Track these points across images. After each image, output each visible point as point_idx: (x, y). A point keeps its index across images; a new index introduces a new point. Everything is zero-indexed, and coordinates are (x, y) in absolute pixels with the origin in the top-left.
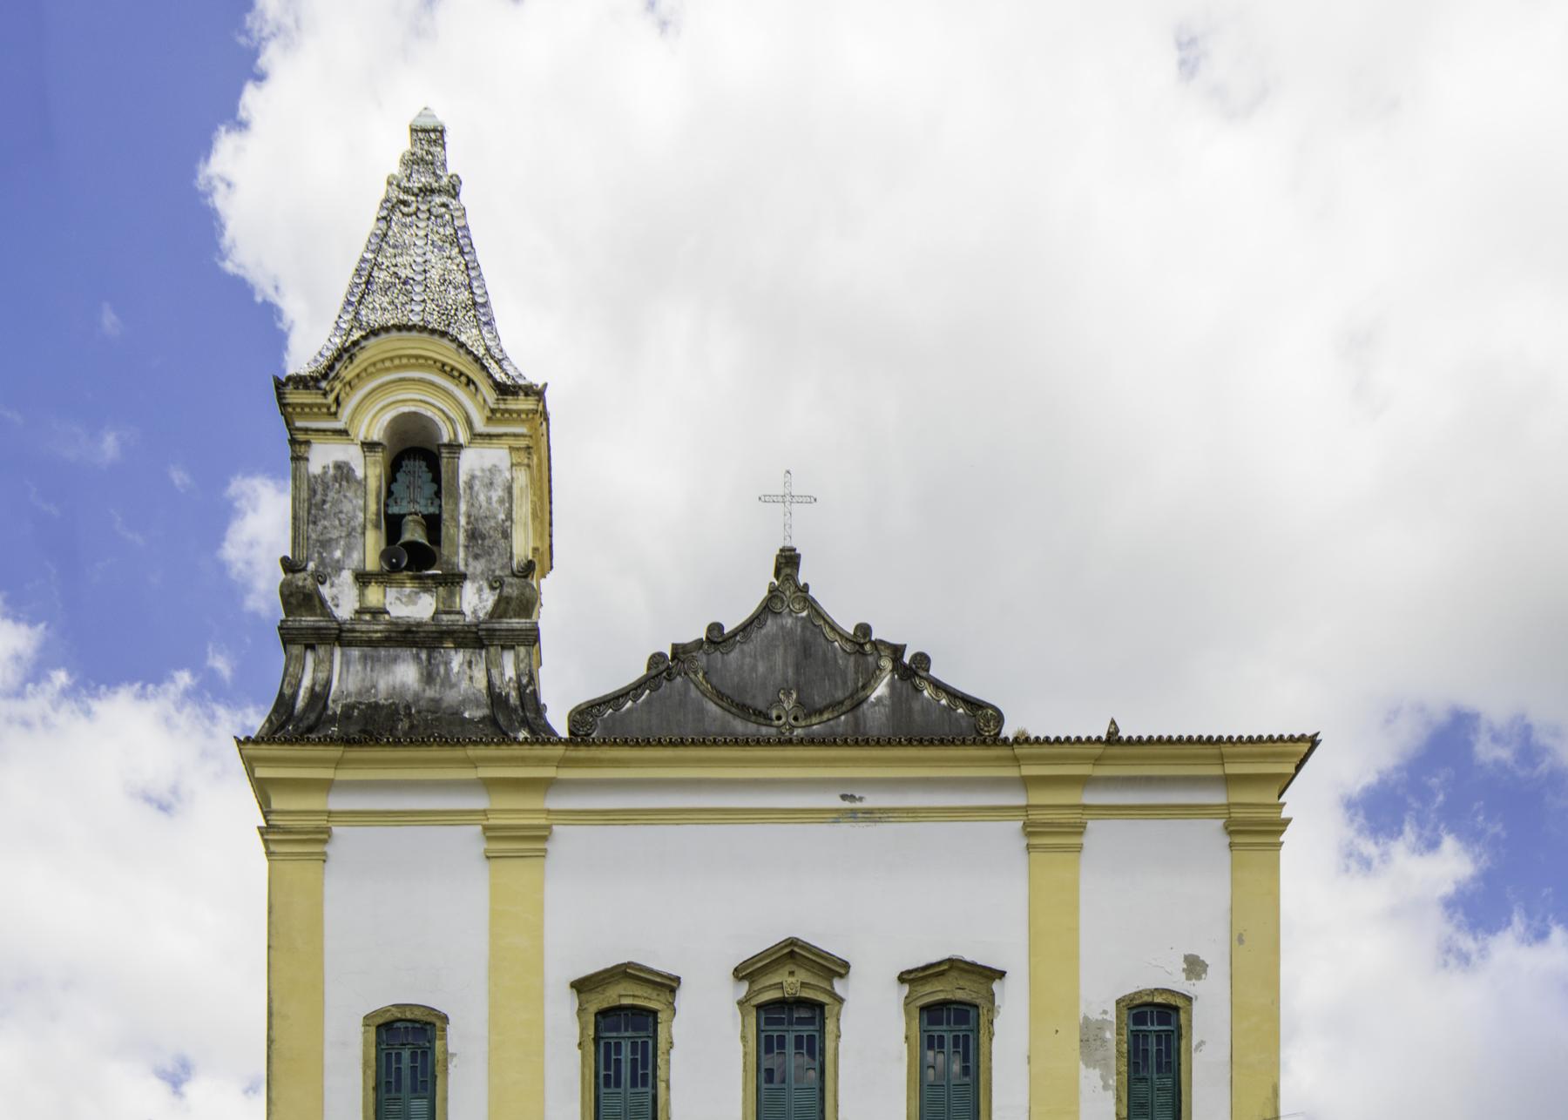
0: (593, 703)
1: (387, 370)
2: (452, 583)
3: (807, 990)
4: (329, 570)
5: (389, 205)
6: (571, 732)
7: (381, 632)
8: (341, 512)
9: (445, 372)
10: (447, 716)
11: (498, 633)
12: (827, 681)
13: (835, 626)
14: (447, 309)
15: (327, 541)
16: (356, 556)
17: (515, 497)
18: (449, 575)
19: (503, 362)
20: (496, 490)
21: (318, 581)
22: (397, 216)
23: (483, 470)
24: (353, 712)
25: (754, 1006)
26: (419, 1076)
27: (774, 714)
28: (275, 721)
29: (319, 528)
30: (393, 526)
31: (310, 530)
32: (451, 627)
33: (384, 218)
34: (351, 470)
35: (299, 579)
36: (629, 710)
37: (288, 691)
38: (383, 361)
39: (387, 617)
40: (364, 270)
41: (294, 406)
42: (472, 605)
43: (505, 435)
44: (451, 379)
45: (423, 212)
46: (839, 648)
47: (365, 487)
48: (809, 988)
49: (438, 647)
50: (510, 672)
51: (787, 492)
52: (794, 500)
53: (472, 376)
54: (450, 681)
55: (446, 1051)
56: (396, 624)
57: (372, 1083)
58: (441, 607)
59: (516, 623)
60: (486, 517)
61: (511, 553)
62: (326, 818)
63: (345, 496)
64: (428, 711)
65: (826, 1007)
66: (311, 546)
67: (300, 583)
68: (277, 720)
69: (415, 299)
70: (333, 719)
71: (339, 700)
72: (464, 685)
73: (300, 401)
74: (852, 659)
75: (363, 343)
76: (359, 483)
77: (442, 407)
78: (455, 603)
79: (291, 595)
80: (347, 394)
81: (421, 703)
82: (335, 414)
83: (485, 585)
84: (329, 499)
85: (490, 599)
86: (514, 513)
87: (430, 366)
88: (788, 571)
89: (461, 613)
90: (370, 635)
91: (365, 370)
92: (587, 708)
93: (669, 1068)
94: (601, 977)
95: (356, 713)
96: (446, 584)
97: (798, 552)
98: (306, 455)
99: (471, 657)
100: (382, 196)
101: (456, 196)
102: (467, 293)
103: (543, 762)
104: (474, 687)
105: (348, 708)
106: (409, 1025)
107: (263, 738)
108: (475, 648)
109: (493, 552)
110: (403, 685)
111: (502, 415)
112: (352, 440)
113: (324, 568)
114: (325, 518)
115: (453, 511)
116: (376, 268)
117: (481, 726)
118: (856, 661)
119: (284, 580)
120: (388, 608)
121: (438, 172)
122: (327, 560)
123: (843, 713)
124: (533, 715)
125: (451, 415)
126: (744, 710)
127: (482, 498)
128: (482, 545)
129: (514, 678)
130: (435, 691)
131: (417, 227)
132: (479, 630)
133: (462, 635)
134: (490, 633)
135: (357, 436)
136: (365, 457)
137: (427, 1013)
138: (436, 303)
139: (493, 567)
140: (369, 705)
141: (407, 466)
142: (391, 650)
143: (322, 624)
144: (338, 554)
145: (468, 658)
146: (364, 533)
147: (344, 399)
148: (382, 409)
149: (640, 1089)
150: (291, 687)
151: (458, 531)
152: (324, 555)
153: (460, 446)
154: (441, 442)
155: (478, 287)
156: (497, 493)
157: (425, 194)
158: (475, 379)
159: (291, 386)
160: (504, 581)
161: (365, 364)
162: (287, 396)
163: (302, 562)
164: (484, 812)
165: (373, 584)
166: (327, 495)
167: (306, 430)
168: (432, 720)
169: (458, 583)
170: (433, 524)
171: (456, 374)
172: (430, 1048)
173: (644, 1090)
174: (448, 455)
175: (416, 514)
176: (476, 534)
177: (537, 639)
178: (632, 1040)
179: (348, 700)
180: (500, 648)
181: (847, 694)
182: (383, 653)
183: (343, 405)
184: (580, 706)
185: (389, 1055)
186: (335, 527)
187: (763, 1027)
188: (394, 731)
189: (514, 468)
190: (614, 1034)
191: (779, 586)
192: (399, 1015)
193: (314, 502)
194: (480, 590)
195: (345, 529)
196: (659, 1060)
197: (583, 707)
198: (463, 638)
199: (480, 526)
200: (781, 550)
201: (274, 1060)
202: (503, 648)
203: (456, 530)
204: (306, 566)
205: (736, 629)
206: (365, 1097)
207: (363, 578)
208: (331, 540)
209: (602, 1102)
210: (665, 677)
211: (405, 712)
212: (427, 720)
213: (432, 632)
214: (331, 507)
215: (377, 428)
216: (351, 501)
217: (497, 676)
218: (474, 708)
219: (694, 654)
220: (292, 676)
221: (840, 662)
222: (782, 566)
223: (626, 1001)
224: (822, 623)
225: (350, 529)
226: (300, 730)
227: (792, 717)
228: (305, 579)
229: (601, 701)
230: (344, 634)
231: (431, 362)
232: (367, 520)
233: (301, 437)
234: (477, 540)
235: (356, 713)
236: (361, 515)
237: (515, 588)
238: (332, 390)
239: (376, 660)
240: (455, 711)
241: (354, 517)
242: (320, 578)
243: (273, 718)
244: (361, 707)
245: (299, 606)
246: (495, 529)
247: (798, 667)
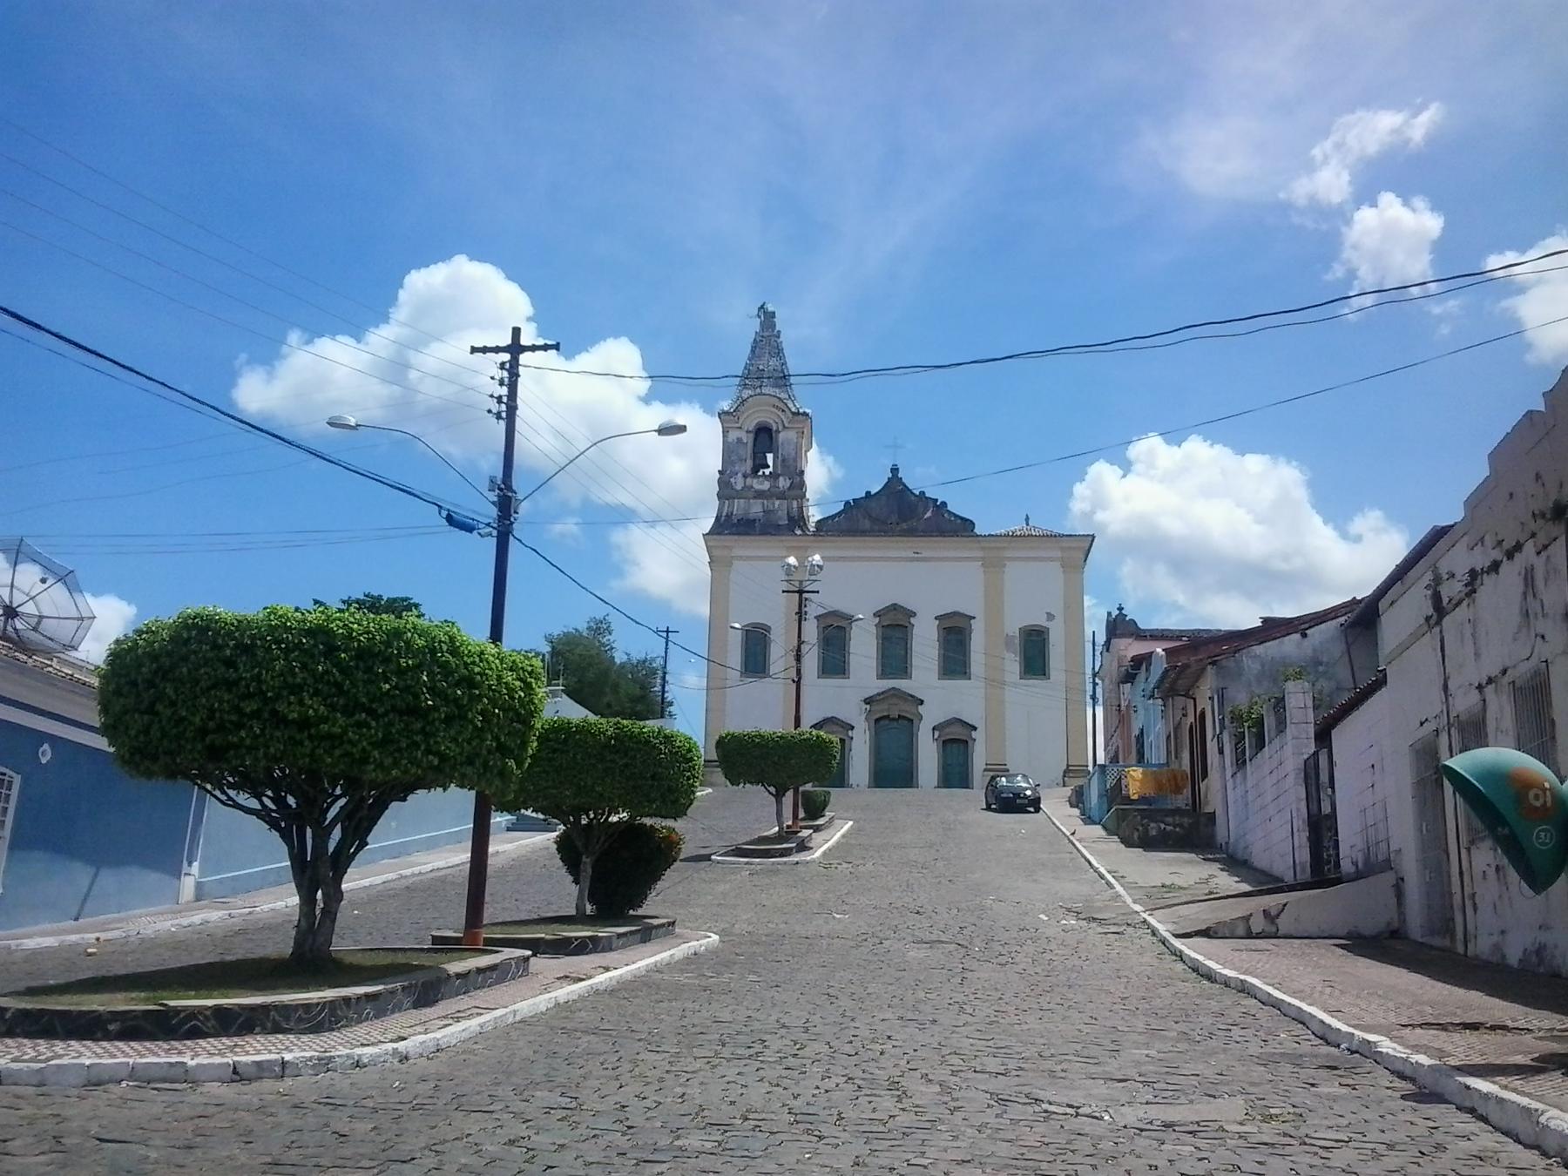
89: (778, 487)
194: (785, 480)
207: (745, 476)
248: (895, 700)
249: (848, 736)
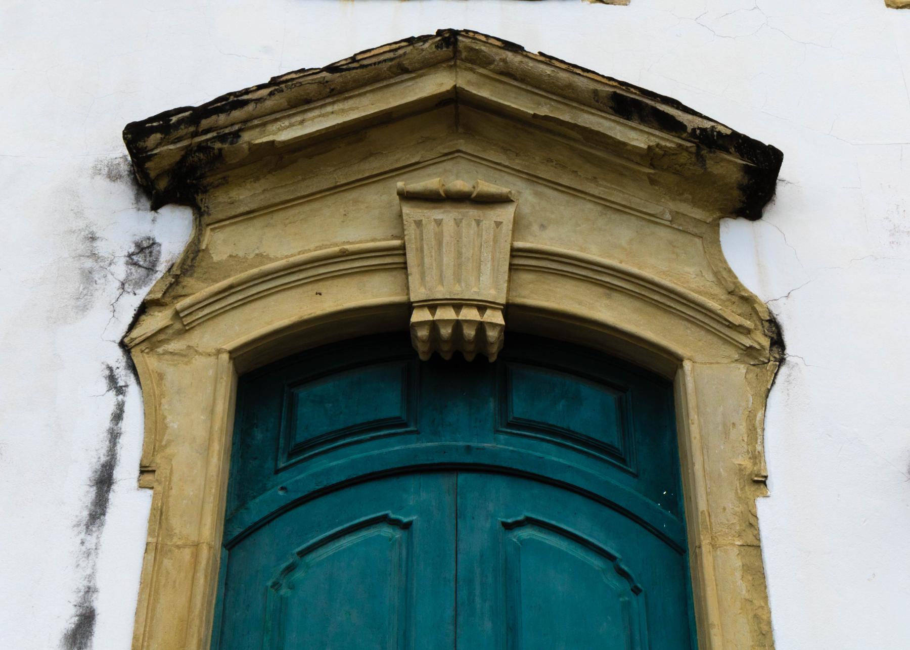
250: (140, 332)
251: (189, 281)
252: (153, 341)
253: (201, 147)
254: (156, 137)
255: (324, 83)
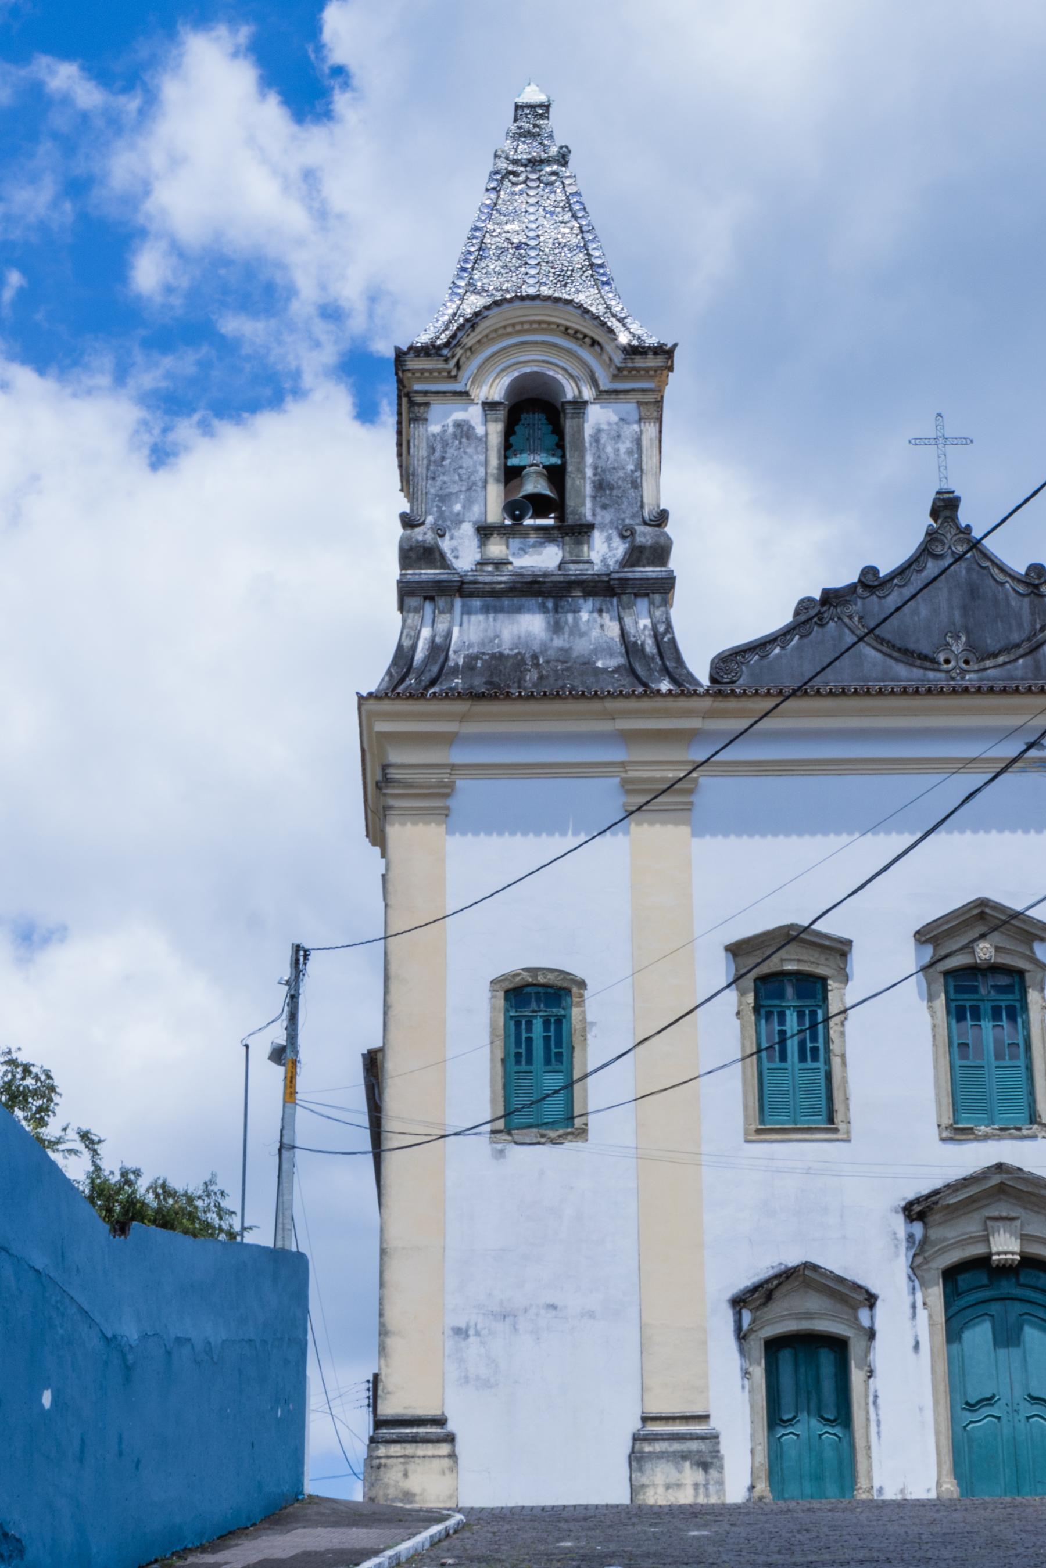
0: (738, 650)
1: (509, 334)
2: (580, 533)
3: (1003, 955)
4: (449, 523)
5: (498, 177)
6: (713, 680)
7: (505, 583)
8: (461, 467)
9: (568, 334)
10: (578, 666)
11: (631, 582)
12: (999, 623)
13: (1005, 568)
14: (562, 271)
15: (446, 495)
16: (476, 510)
17: (644, 449)
18: (577, 525)
19: (626, 321)
20: (624, 442)
21: (438, 534)
22: (506, 183)
23: (609, 424)
24: (476, 663)
25: (940, 972)
26: (553, 1046)
27: (941, 658)
28: (396, 675)
29: (438, 483)
30: (511, 475)
31: (428, 486)
32: (580, 577)
33: (494, 189)
34: (471, 428)
35: (420, 534)
36: (778, 656)
37: (407, 643)
38: (505, 327)
39: (510, 567)
40: (476, 238)
41: (413, 372)
42: (601, 554)
43: (633, 390)
44: (574, 340)
45: (533, 180)
46: (1010, 589)
47: (486, 443)
48: (1005, 953)
49: (566, 596)
50: (645, 622)
51: (940, 434)
52: (948, 443)
53: (596, 337)
54: (579, 630)
55: (584, 1020)
56: (521, 575)
57: (500, 1054)
58: (568, 558)
59: (650, 571)
60: (614, 468)
61: (642, 502)
62: (449, 771)
63: (465, 453)
64: (557, 661)
65: (1027, 975)
66: (430, 501)
67: (420, 538)
68: (397, 673)
69: (529, 262)
70: (455, 671)
71: (460, 651)
72: (595, 633)
73: (421, 367)
74: (1026, 600)
75: (486, 313)
76: (480, 439)
77: (564, 365)
78: (582, 551)
79: (411, 549)
80: (468, 358)
81: (549, 653)
82: (455, 377)
83: (614, 534)
84: (448, 455)
85: (620, 549)
86: (644, 463)
87: (552, 330)
88: (947, 513)
89: (589, 562)
90: (494, 586)
91: (487, 336)
92: (731, 655)
93: (844, 1041)
94: (760, 940)
95: (479, 664)
96: (573, 534)
97: (956, 494)
98: (425, 415)
99: (601, 605)
100: (491, 169)
101: (565, 164)
102: (581, 255)
103: (688, 713)
104: (606, 635)
105: (471, 659)
106: (541, 990)
107: (386, 694)
108: (605, 596)
109: (623, 502)
110: (529, 634)
111: (630, 372)
112: (473, 400)
113: (443, 522)
114: (444, 474)
115: (579, 463)
116: (487, 235)
117: (616, 676)
118: (1031, 603)
119: (403, 534)
120: (511, 559)
121: (546, 142)
122: (447, 514)
123: (1021, 657)
124: (674, 665)
125: (575, 373)
126: (908, 655)
127: (609, 449)
128: (610, 495)
129: (650, 626)
130: (564, 641)
131: (528, 195)
132: (611, 579)
133: (592, 584)
134: (623, 582)
135: (478, 396)
136: (486, 415)
137: (562, 977)
138: (551, 265)
139: (623, 516)
140: (493, 656)
141: (526, 419)
142: (516, 600)
143: (443, 577)
144: (458, 507)
145: (598, 605)
146: (485, 487)
147: (464, 363)
148: (503, 370)
149: (810, 1064)
150: (410, 639)
151: (585, 481)
152: (444, 508)
153: (585, 403)
154: (565, 400)
155: (594, 249)
156: (624, 446)
157: (534, 165)
158: (601, 340)
159: (412, 354)
160: (635, 531)
161: (485, 332)
162: (408, 363)
163: (421, 516)
164: (623, 764)
165: (495, 536)
166: (446, 452)
167: (426, 393)
168: (563, 670)
169: (586, 533)
170: (556, 475)
171: (580, 336)
172: (564, 1016)
173: (815, 1065)
174: (572, 411)
175: (537, 465)
176: (604, 484)
177: (672, 586)
178: (798, 1009)
179: (471, 651)
180: (633, 596)
181: (1024, 636)
182: (506, 602)
183: (463, 368)
184: (723, 652)
185: (518, 1024)
186: (454, 482)
187: (952, 996)
188: (522, 682)
189: (643, 421)
190: (776, 1002)
191: (939, 528)
192: (530, 980)
193: (433, 459)
194: (609, 539)
195: (465, 483)
196: (831, 1032)
197: (727, 653)
198: (593, 587)
199: (608, 476)
200: (938, 493)
201: (392, 1027)
202: (636, 595)
203: (582, 481)
204: (424, 521)
205: (893, 571)
206: (493, 1068)
207: (485, 532)
208: (450, 494)
209: (766, 1079)
210: (816, 623)
211: (532, 661)
212: (558, 670)
213: (560, 582)
214: (450, 463)
215: (499, 388)
216: (471, 457)
217: (631, 625)
218: (608, 657)
219: (848, 598)
220: (410, 628)
221: (1013, 603)
222: (941, 509)
223: (789, 967)
224: (988, 564)
225: (470, 484)
226: (423, 684)
227: (962, 661)
228: (425, 534)
229: (746, 648)
230: (465, 586)
231: (554, 327)
232: (489, 475)
233: (419, 399)
234: (604, 490)
235: (479, 664)
236: (481, 471)
237: (648, 537)
238: (453, 356)
239: (498, 610)
240: (586, 660)
241: (474, 472)
242: (440, 533)
243: (393, 671)
244: (484, 657)
245: (419, 559)
246: (624, 480)
247: (965, 610)
248: (1002, 1209)
249: (859, 1327)
250: (915, 1264)
251: (926, 1247)
252: (919, 1266)
253: (928, 1207)
254: (916, 1205)
255: (963, 1184)
